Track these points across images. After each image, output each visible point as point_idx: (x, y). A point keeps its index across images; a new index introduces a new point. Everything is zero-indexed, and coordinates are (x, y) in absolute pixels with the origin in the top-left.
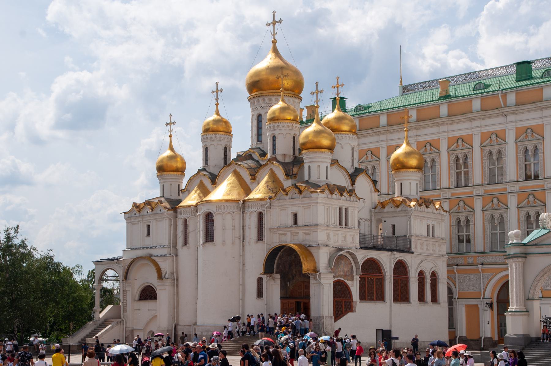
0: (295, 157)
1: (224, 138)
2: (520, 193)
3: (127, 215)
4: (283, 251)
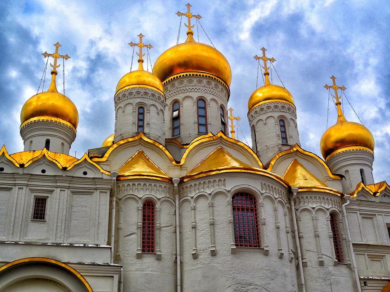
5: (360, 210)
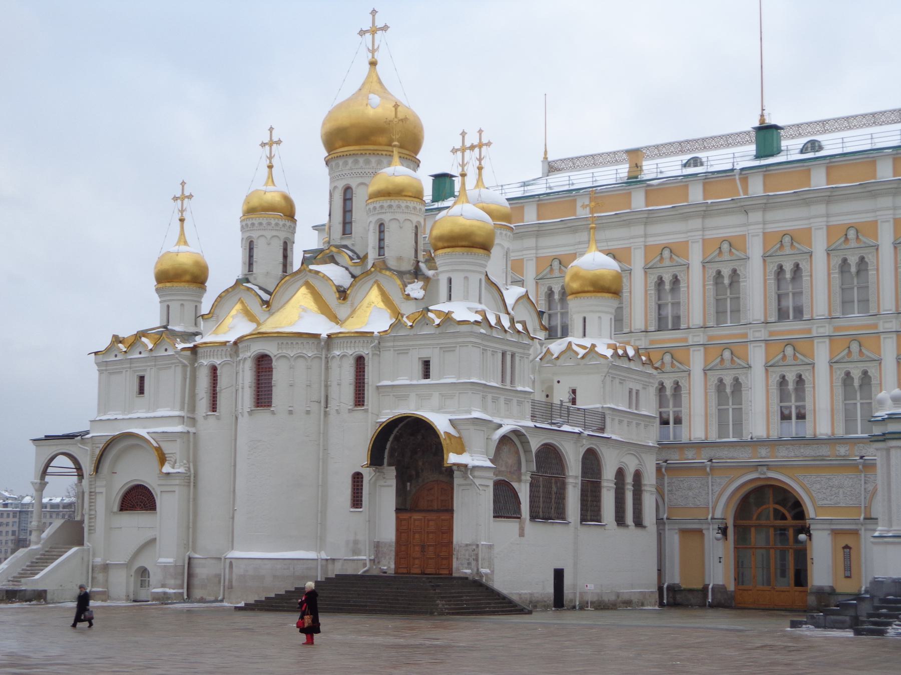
1: (284, 225)
2: (771, 342)
3: (100, 357)
4: (402, 427)
5: (393, 347)
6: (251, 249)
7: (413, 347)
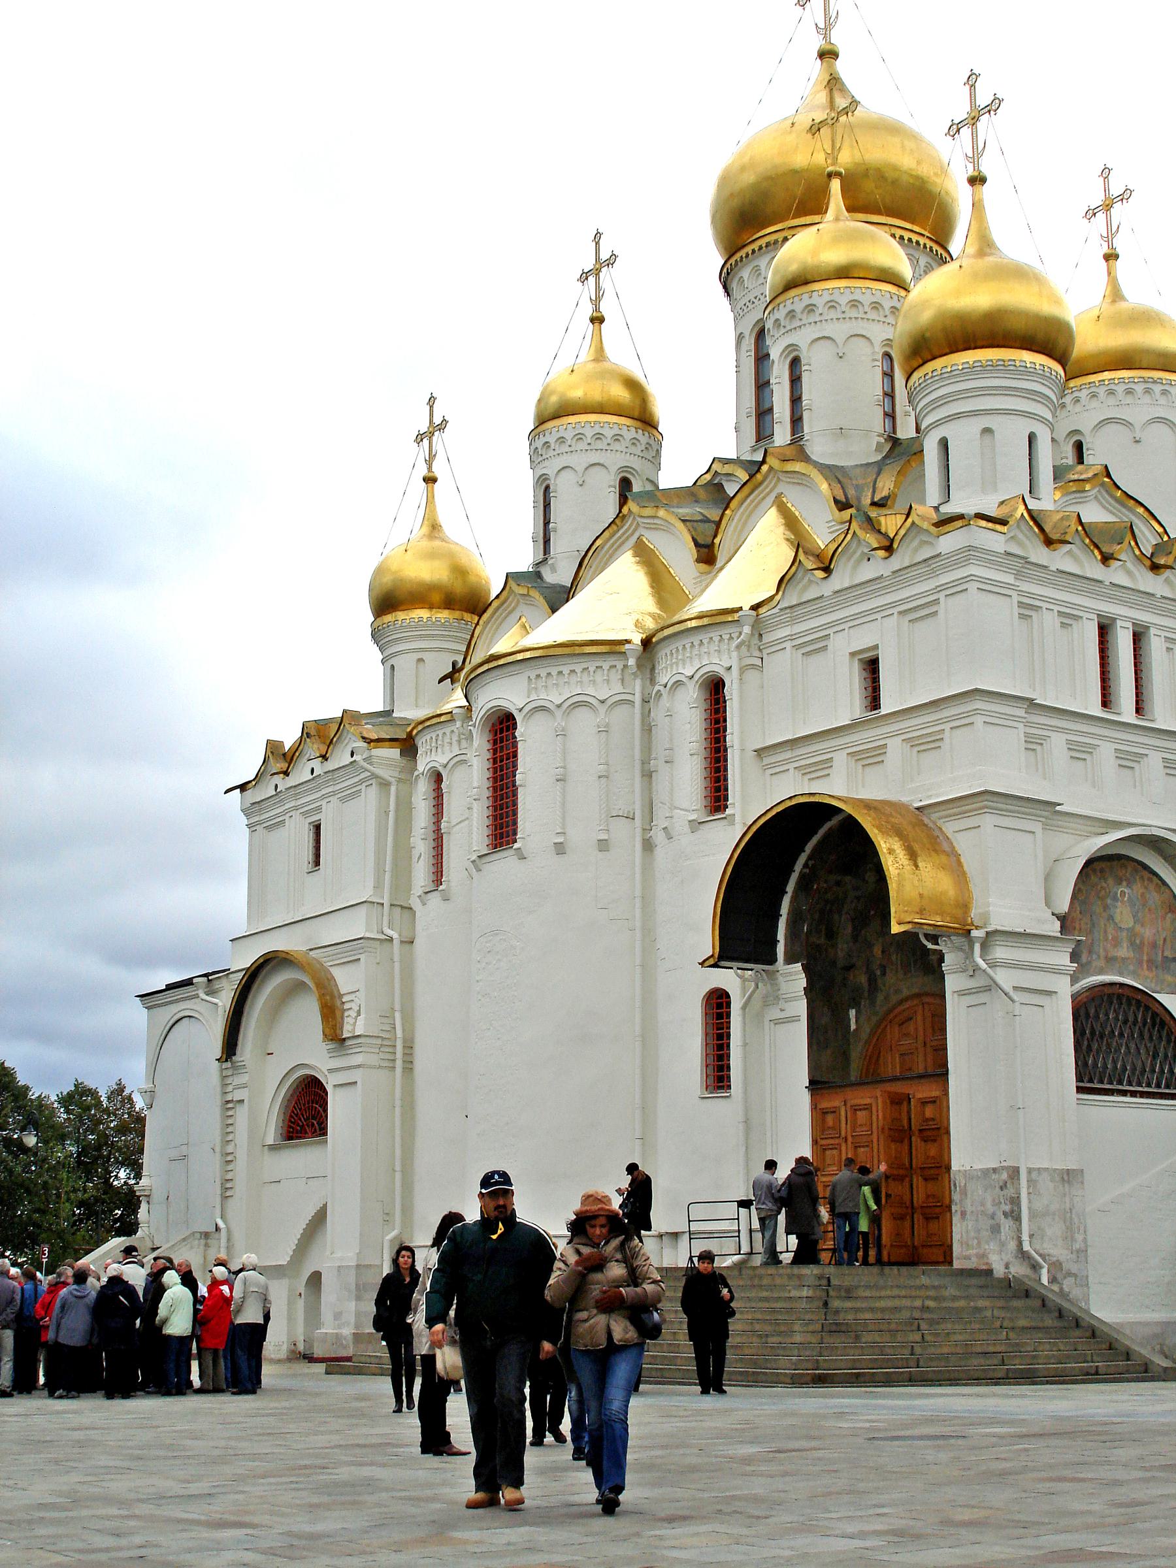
0: (895, 442)
1: (617, 438)
6: (547, 506)
7: (835, 629)
